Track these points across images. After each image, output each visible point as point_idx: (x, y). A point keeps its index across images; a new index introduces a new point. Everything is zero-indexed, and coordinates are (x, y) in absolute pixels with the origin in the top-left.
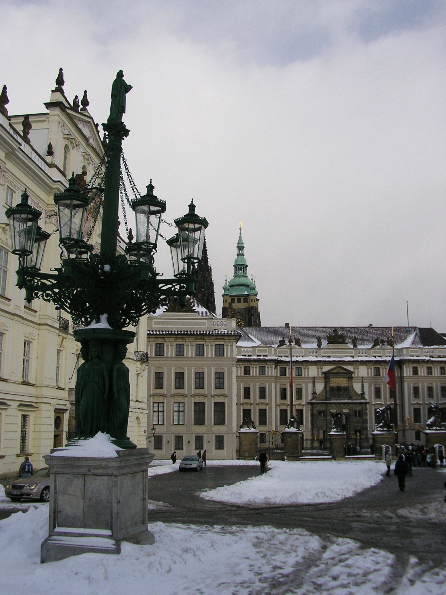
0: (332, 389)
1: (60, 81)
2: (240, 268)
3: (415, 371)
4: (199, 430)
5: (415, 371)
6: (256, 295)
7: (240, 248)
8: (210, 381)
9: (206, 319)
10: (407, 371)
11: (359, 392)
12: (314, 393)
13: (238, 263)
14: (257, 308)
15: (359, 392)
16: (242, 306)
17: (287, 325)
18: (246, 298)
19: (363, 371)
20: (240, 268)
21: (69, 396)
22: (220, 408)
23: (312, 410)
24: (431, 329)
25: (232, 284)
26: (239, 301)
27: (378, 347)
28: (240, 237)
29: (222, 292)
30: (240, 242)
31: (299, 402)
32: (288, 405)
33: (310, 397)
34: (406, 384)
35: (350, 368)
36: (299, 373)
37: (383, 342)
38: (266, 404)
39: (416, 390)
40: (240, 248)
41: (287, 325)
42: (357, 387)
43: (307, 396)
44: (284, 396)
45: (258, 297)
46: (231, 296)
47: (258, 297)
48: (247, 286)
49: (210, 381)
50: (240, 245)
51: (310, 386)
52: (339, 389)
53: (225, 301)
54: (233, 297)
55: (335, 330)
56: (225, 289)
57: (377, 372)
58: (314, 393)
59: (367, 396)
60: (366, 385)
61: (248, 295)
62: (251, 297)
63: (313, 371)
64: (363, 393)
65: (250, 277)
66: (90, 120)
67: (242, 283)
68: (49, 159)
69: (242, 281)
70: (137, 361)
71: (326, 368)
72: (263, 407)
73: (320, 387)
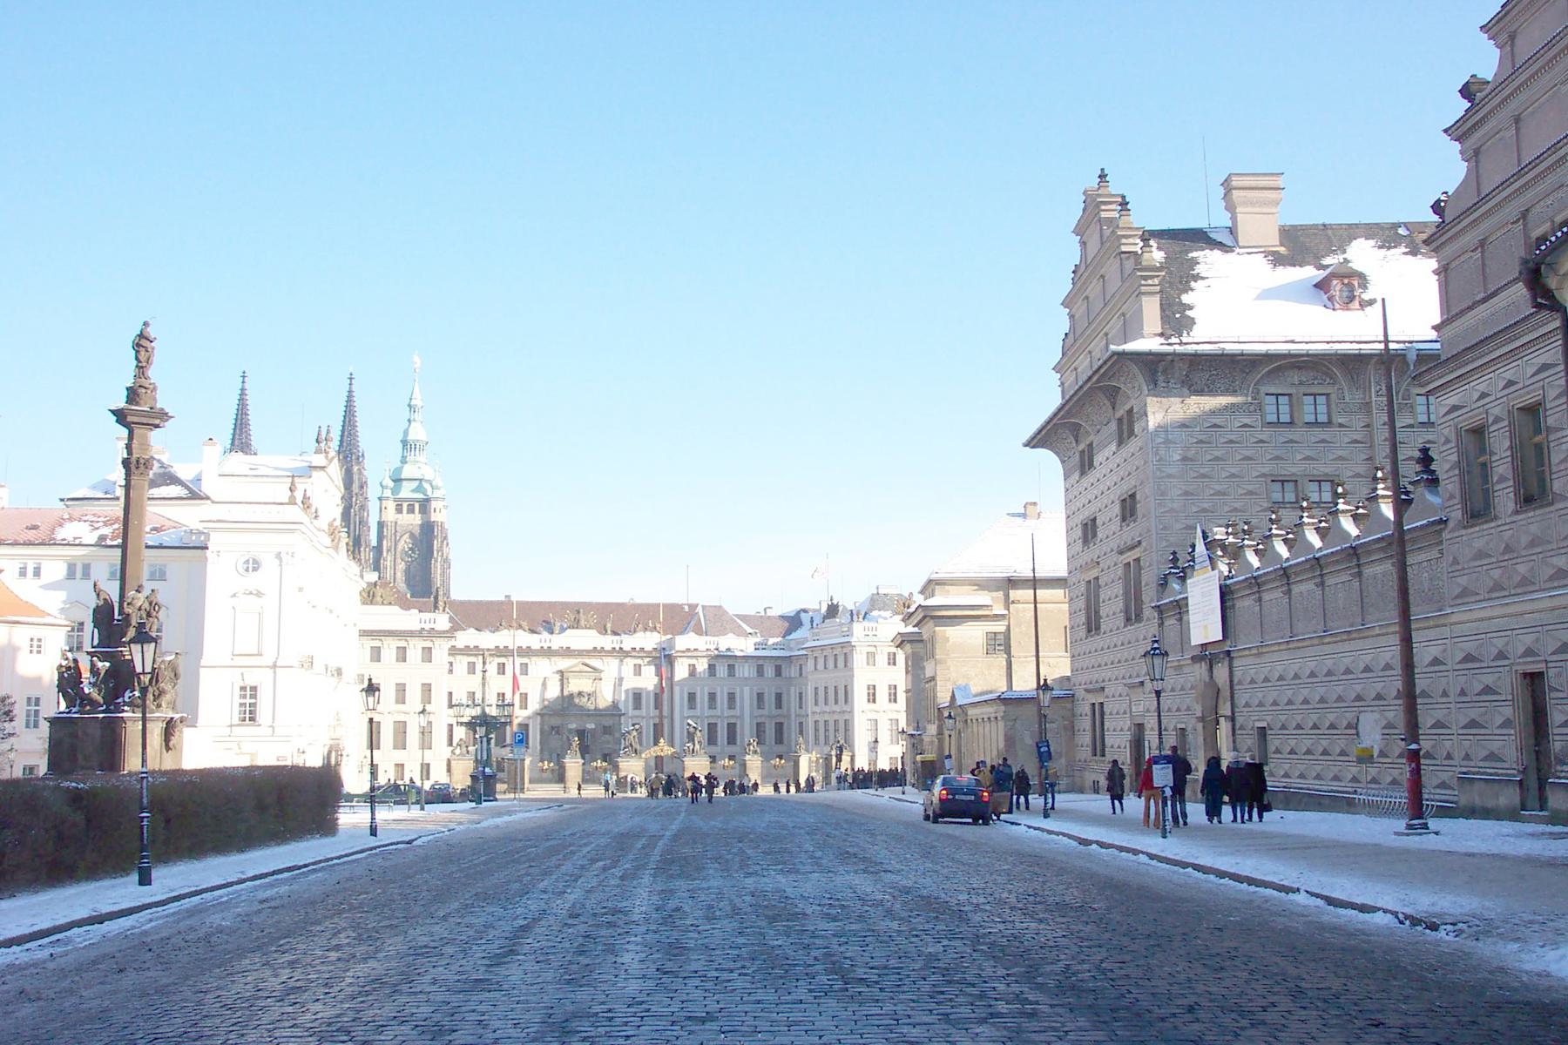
23: (542, 724)
26: (411, 510)
36: (525, 669)
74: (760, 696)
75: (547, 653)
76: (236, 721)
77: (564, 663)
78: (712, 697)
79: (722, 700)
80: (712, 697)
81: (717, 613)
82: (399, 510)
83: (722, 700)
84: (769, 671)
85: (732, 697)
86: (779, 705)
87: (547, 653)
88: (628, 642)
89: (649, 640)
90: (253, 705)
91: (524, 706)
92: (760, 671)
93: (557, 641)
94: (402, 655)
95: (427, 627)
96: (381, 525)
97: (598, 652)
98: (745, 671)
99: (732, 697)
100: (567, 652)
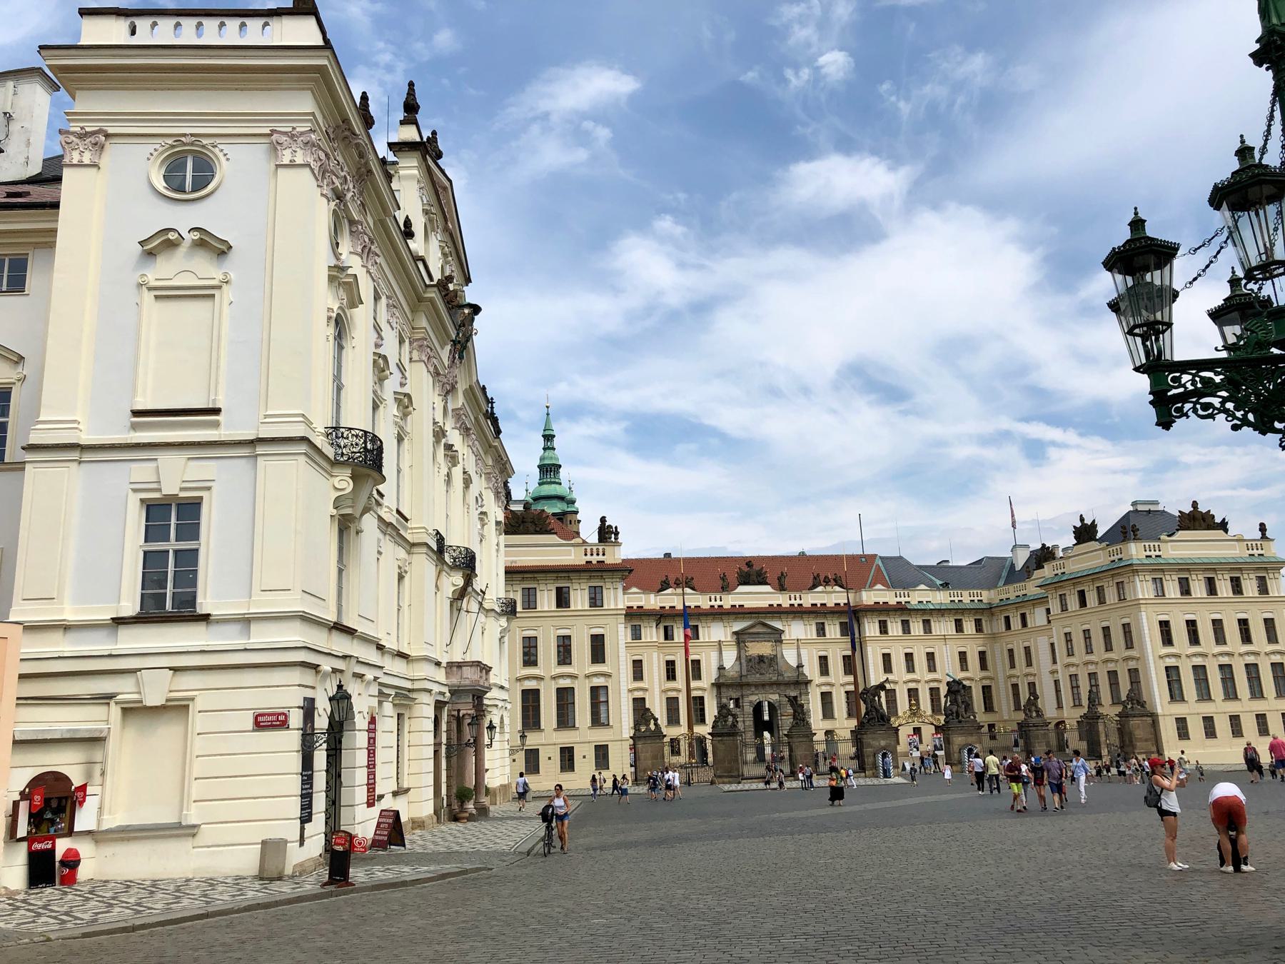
0: (749, 660)
2: (549, 470)
3: (883, 629)
4: (566, 738)
5: (883, 629)
6: (576, 513)
7: (548, 438)
8: (582, 649)
9: (573, 545)
10: (870, 628)
11: (793, 662)
12: (721, 668)
13: (547, 462)
15: (793, 662)
19: (797, 630)
20: (549, 470)
21: (447, 678)
22: (598, 696)
23: (719, 696)
24: (901, 557)
25: (536, 495)
27: (820, 589)
28: (547, 422)
32: (679, 691)
34: (869, 649)
35: (777, 624)
37: (827, 582)
38: (645, 690)
39: (887, 658)
40: (548, 438)
42: (790, 656)
43: (709, 674)
44: (671, 675)
45: (579, 517)
47: (579, 517)
48: (561, 498)
49: (582, 649)
50: (547, 433)
51: (714, 655)
52: (761, 659)
55: (749, 562)
57: (821, 631)
58: (721, 668)
59: (806, 670)
60: (803, 652)
61: (564, 513)
62: (569, 517)
63: (716, 632)
64: (800, 666)
65: (565, 485)
66: (447, 184)
67: (553, 493)
70: (499, 615)
71: (738, 626)
73: (730, 657)
74: (963, 655)
75: (718, 614)
76: (130, 607)
77: (738, 626)
78: (909, 657)
79: (920, 662)
80: (909, 657)
81: (897, 563)
83: (920, 662)
84: (969, 627)
85: (931, 657)
86: (984, 666)
87: (718, 614)
88: (808, 599)
89: (833, 597)
90: (188, 559)
92: (959, 627)
93: (728, 601)
94: (562, 600)
95: (595, 559)
97: (776, 612)
98: (944, 627)
99: (931, 657)
100: (737, 613)
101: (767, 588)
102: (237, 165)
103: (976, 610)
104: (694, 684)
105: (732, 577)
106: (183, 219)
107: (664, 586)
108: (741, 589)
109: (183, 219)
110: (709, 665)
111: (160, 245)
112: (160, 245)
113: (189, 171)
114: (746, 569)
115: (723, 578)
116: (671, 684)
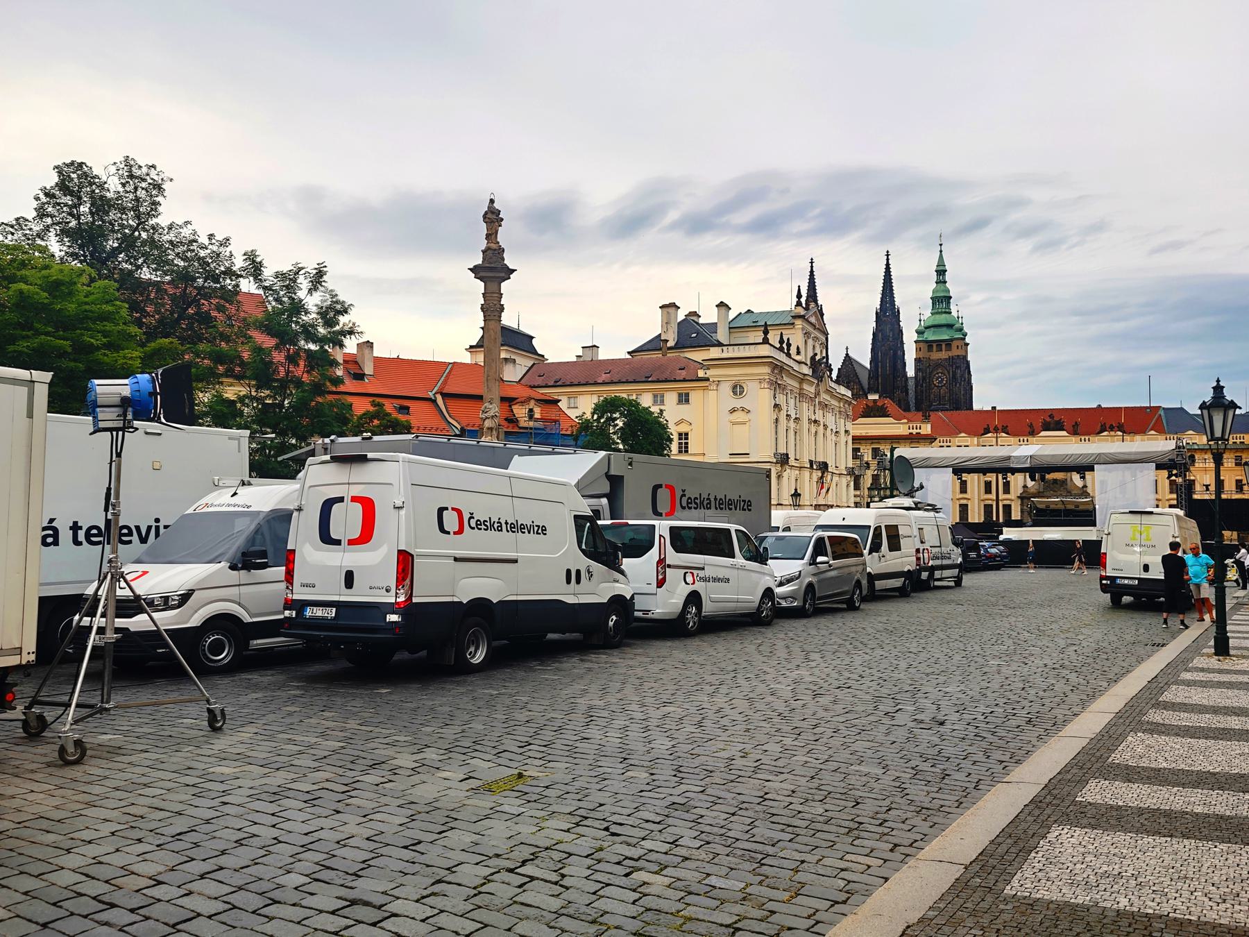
1: (799, 296)
2: (941, 301)
7: (941, 272)
14: (965, 357)
16: (944, 355)
17: (994, 408)
18: (948, 343)
20: (941, 301)
23: (1022, 505)
28: (941, 256)
29: (915, 337)
30: (941, 263)
31: (1007, 496)
33: (1020, 491)
37: (1112, 428)
40: (941, 272)
41: (994, 408)
46: (926, 342)
48: (950, 326)
53: (918, 350)
54: (930, 344)
55: (1051, 413)
56: (919, 332)
58: (1025, 486)
61: (952, 340)
62: (954, 344)
64: (1085, 486)
65: (954, 314)
67: (944, 322)
68: (798, 358)
69: (942, 319)
72: (964, 502)
82: (930, 348)
91: (1007, 491)
95: (914, 431)
96: (917, 360)
101: (1064, 433)
102: (751, 387)
103: (1237, 450)
104: (1001, 496)
105: (1038, 424)
106: (738, 403)
107: (987, 431)
108: (1043, 433)
109: (738, 403)
110: (1016, 485)
111: (733, 411)
112: (733, 411)
113: (738, 390)
114: (1048, 419)
115: (1031, 426)
116: (988, 496)
